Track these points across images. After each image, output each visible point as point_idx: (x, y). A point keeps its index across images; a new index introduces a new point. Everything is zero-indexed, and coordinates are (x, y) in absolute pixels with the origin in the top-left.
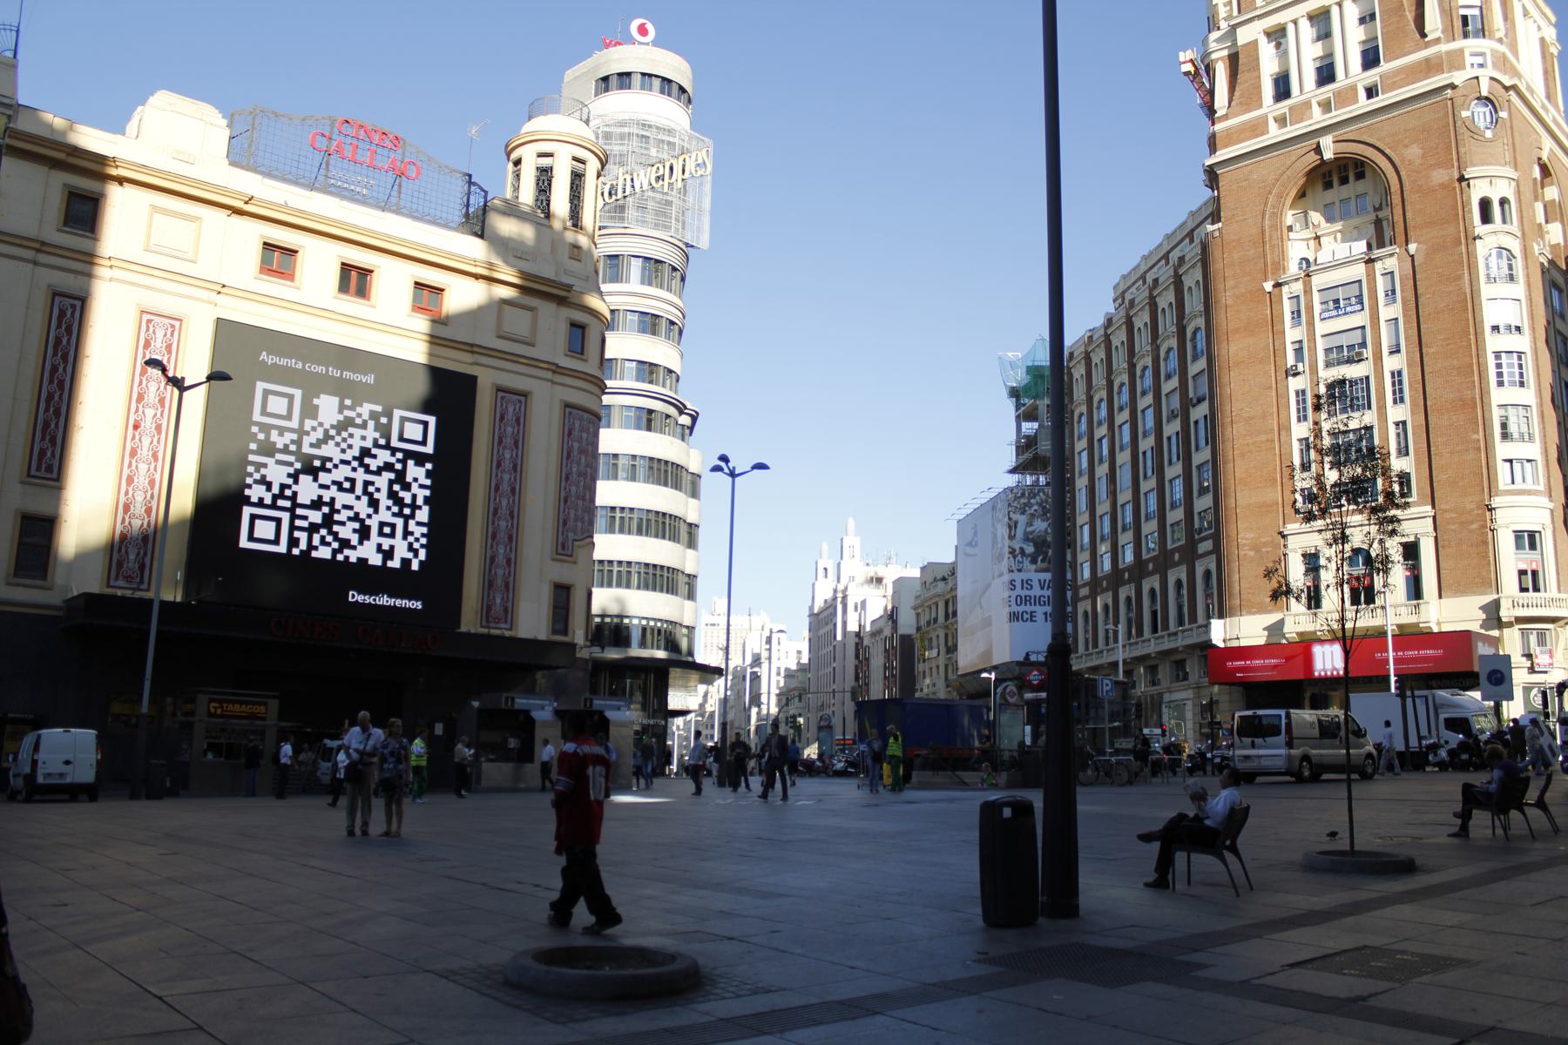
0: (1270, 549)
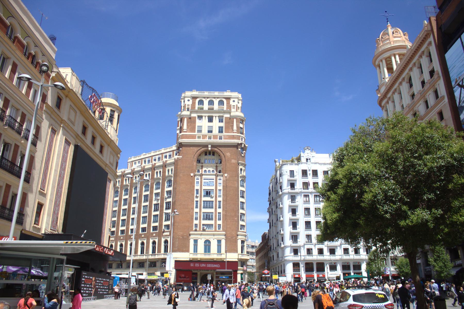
0: (186, 237)
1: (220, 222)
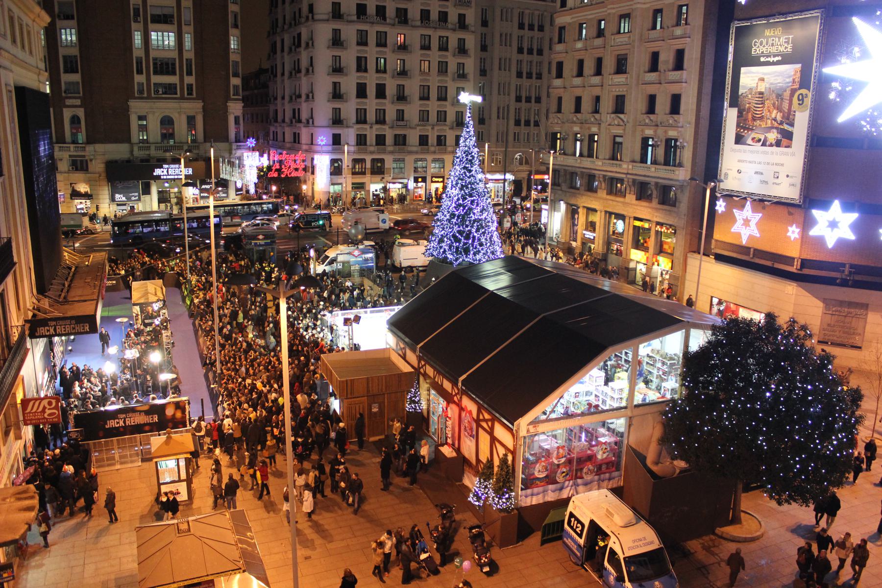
1: (190, 80)
